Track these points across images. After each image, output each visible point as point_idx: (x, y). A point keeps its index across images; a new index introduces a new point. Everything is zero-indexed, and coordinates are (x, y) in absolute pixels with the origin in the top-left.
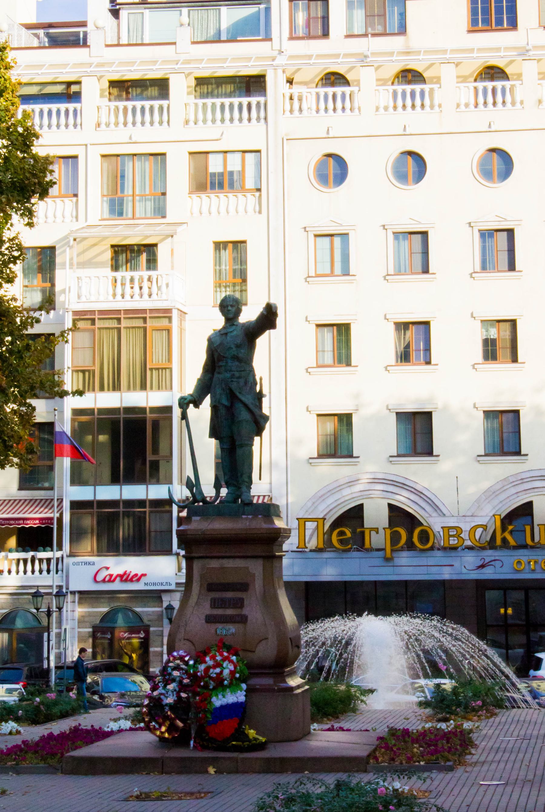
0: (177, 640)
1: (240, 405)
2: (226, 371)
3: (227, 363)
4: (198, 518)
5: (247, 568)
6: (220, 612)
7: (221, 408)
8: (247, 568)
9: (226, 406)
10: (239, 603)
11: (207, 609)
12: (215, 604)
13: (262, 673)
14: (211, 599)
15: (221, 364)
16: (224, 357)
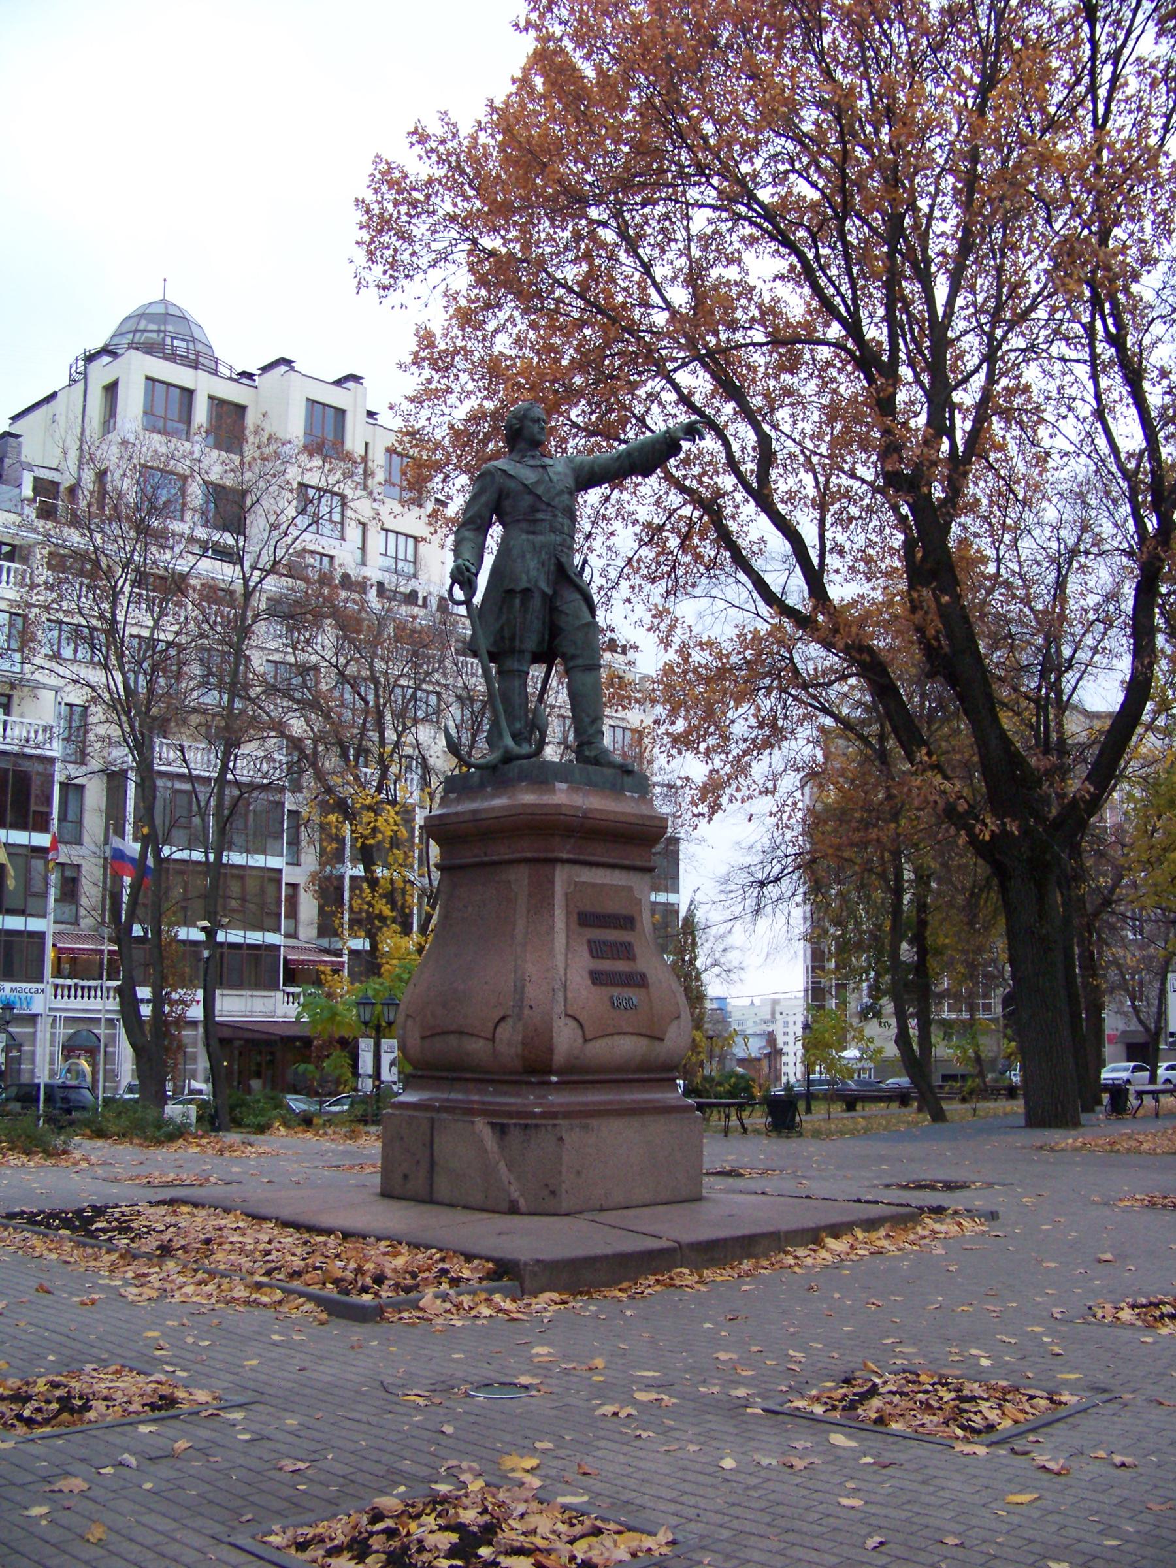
0: (555, 1017)
1: (578, 596)
2: (553, 530)
3: (555, 516)
4: (564, 786)
5: (630, 889)
6: (606, 965)
7: (537, 594)
8: (630, 889)
9: (544, 594)
10: (626, 951)
11: (583, 962)
12: (597, 950)
13: (624, 1081)
14: (589, 942)
15: (540, 516)
16: (548, 505)
